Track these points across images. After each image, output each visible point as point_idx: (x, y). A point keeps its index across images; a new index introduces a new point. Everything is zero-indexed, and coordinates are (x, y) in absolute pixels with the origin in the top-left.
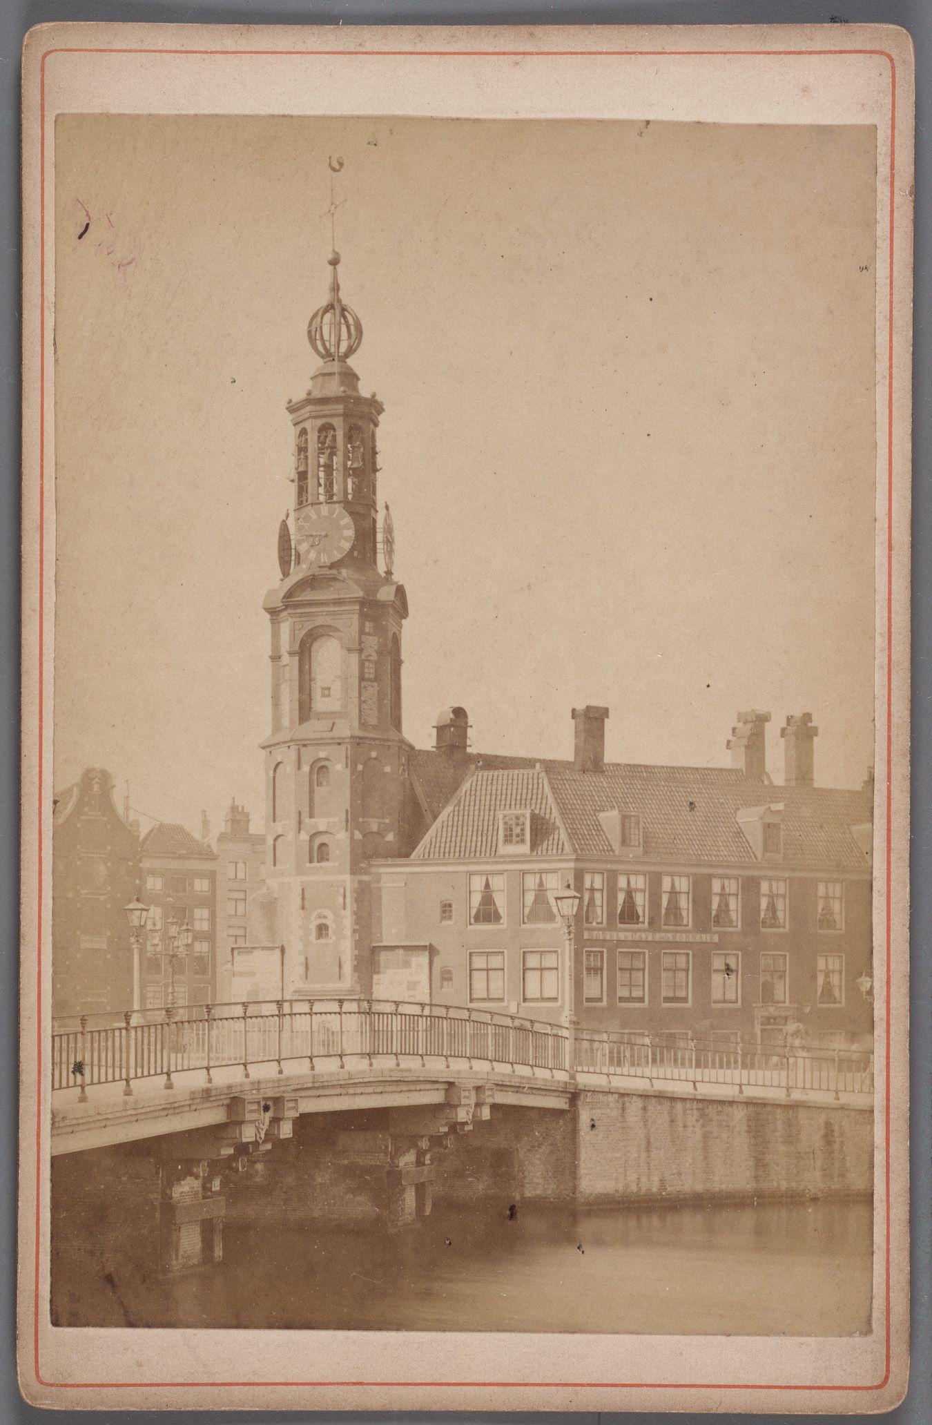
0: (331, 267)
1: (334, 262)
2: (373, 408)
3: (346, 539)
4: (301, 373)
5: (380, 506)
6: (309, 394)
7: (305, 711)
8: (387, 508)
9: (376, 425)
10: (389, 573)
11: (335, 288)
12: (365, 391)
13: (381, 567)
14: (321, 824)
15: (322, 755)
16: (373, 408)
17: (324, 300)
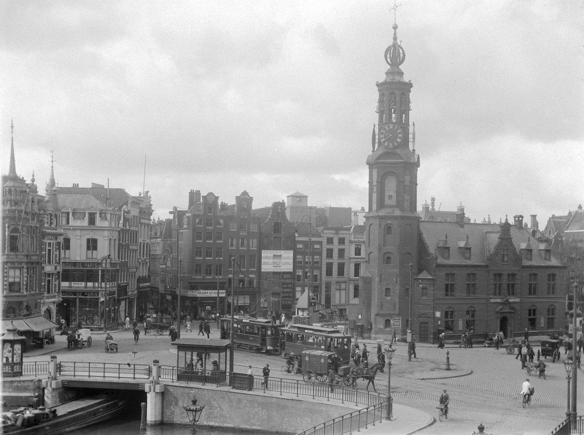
1: (395, 28)
2: (410, 85)
3: (400, 138)
4: (380, 71)
5: (411, 124)
6: (386, 80)
7: (381, 204)
8: (414, 125)
9: (410, 92)
10: (414, 150)
11: (395, 39)
12: (406, 78)
13: (411, 148)
14: (389, 248)
15: (389, 222)
16: (410, 85)
17: (390, 42)
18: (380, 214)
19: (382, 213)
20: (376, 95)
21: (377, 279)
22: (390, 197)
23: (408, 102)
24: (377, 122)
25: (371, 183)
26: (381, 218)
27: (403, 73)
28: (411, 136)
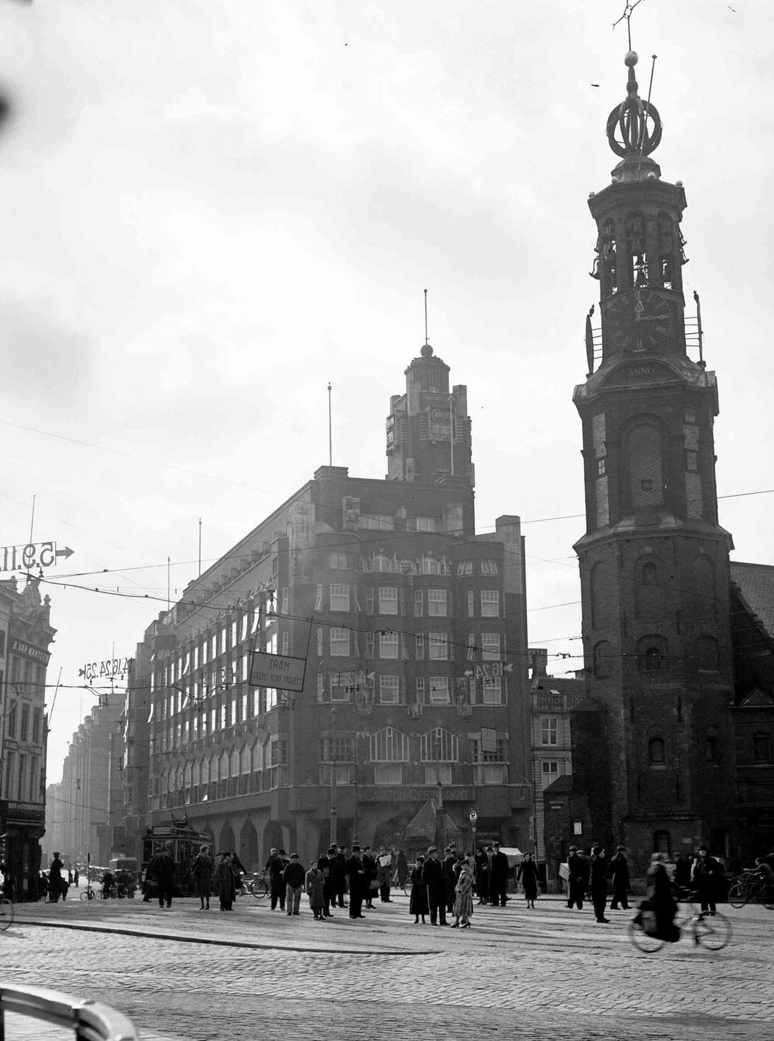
0: (628, 68)
1: (631, 61)
8: (696, 297)
10: (702, 363)
11: (632, 86)
15: (648, 550)
17: (622, 96)
18: (620, 529)
19: (626, 526)
20: (589, 231)
21: (623, 713)
22: (646, 485)
23: (679, 242)
24: (595, 297)
25: (588, 453)
26: (624, 540)
27: (658, 167)
28: (690, 328)
